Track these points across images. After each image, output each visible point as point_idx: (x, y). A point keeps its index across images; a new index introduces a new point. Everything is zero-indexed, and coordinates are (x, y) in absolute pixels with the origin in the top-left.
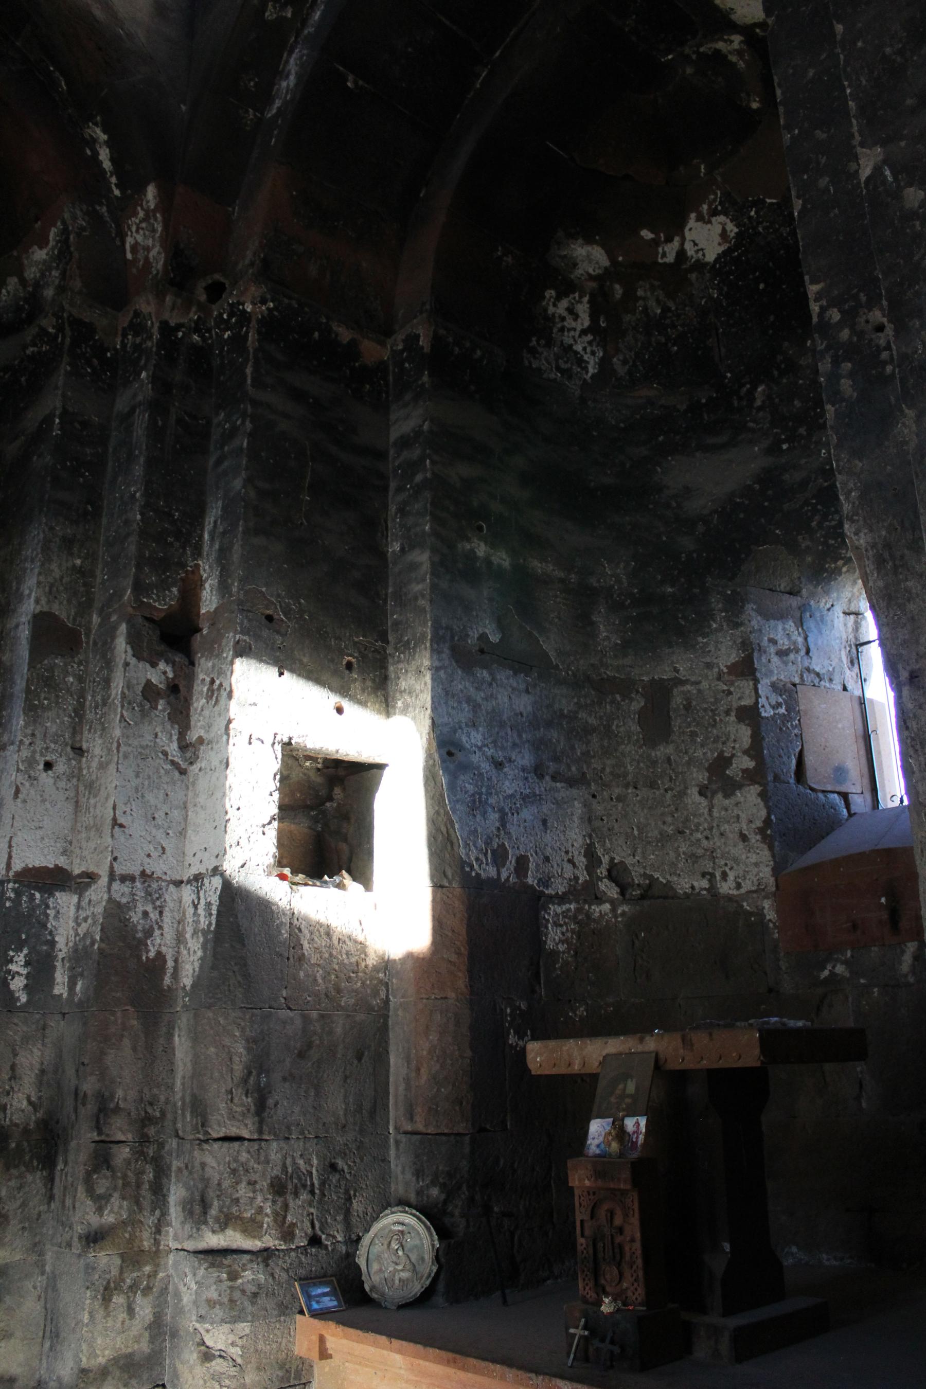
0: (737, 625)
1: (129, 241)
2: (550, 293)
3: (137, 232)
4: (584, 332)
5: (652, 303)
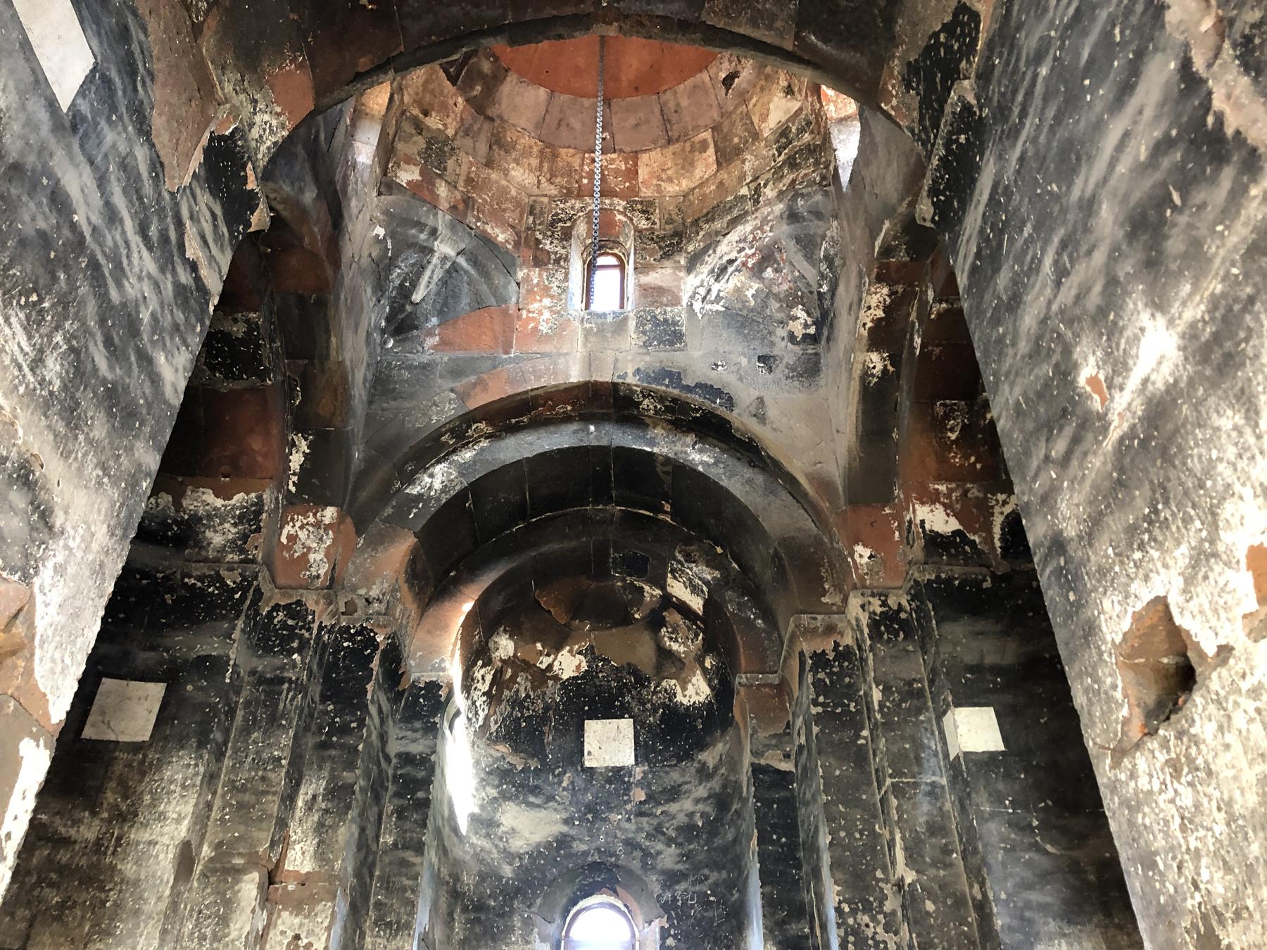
0: (528, 943)
1: (288, 529)
2: (480, 663)
3: (301, 528)
4: (484, 694)
5: (522, 689)
